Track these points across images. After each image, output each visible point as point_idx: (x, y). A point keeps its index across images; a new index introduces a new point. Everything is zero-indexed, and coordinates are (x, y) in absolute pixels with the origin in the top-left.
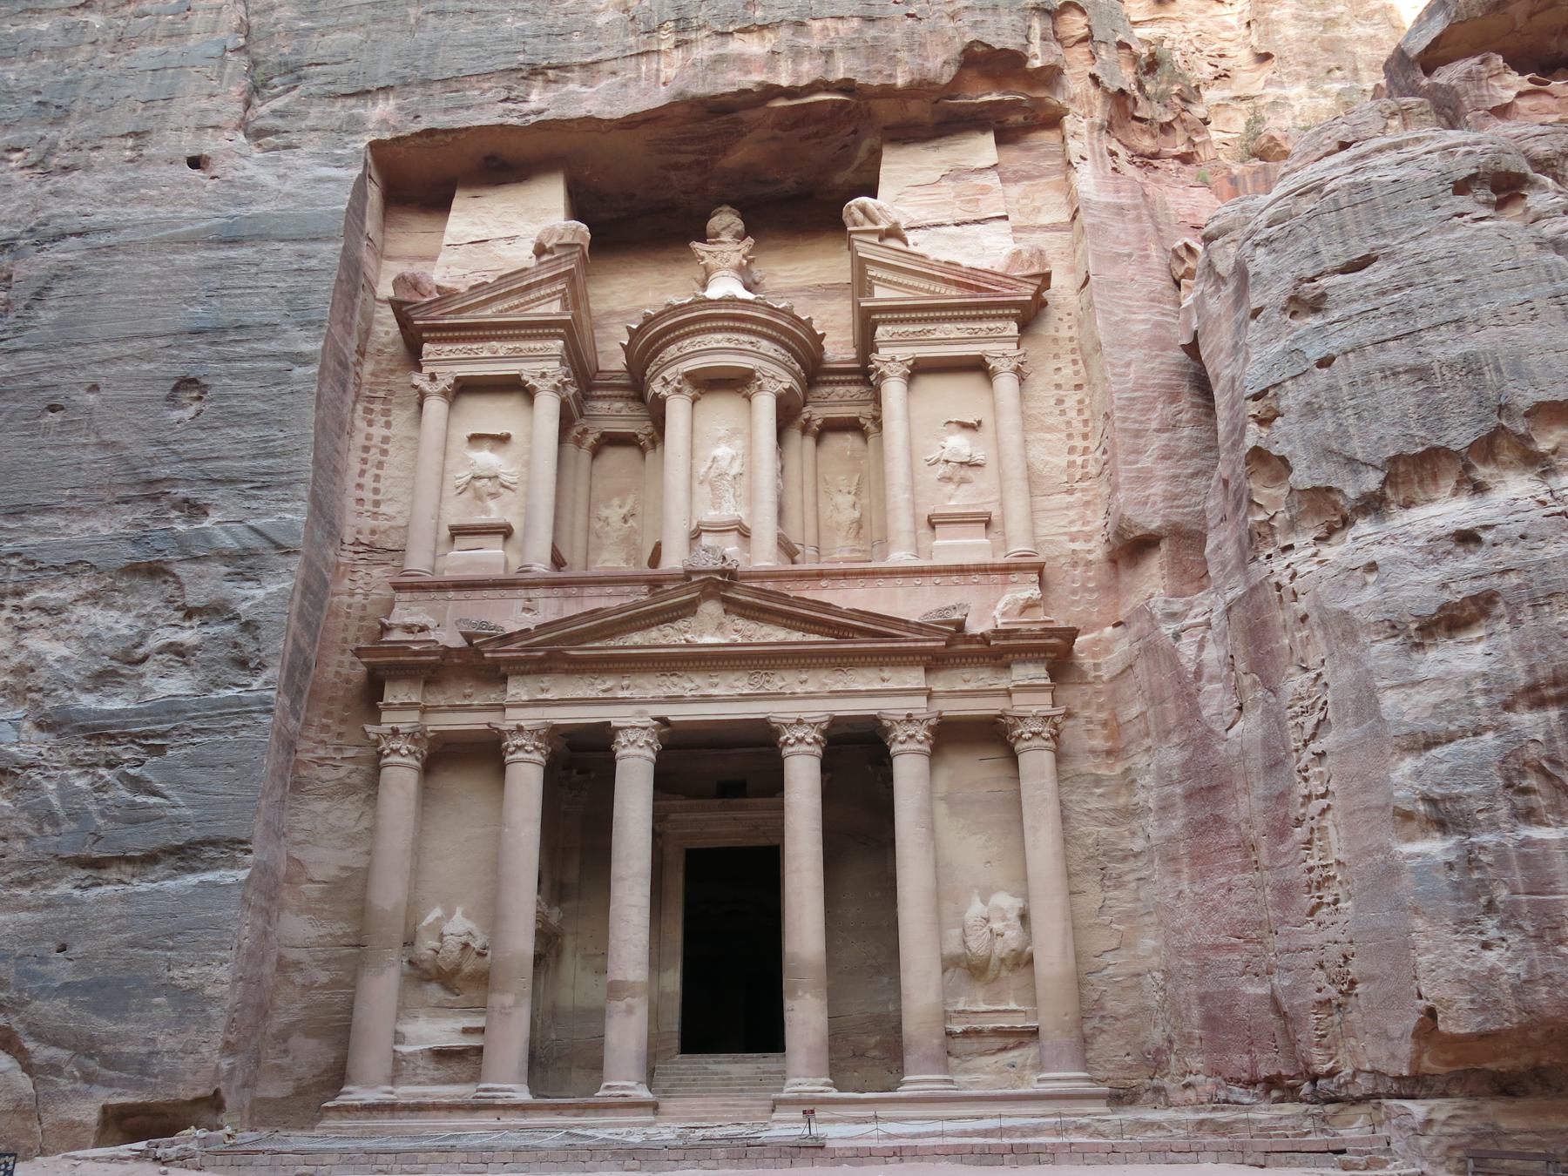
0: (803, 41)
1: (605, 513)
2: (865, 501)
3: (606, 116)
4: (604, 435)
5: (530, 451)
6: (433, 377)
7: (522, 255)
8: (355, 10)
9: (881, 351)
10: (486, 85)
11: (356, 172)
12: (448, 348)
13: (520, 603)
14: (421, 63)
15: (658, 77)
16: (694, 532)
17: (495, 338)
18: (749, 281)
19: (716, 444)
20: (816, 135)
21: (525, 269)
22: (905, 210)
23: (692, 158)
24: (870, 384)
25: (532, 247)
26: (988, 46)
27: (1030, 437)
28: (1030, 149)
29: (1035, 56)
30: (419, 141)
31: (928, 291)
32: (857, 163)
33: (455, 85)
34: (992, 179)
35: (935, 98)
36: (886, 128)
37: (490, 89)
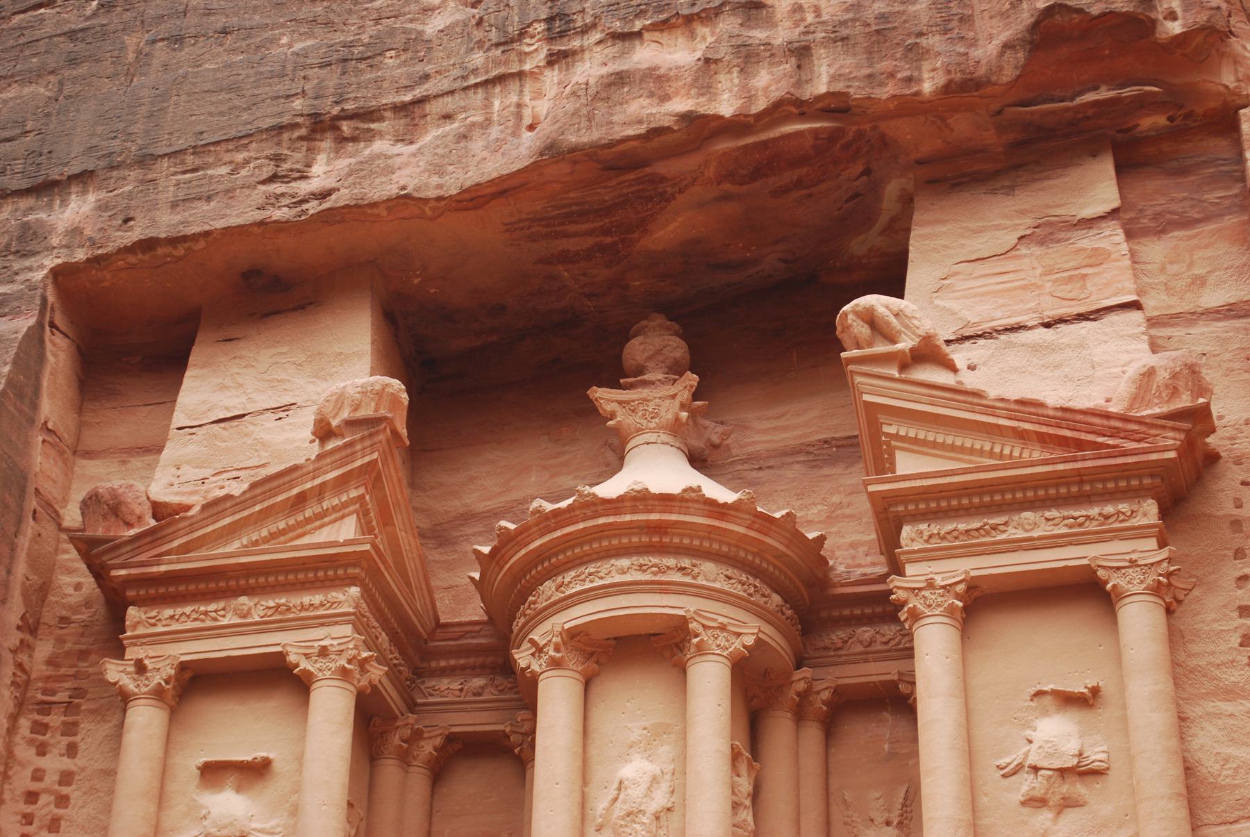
0: (758, 35)
3: (432, 193)
4: (451, 738)
5: (297, 788)
6: (141, 668)
7: (293, 442)
8: (42, 46)
9: (910, 569)
10: (240, 157)
11: (25, 323)
12: (168, 612)
14: (137, 128)
15: (519, 117)
17: (249, 591)
18: (697, 443)
19: (625, 758)
20: (799, 184)
21: (295, 468)
23: (590, 241)
25: (311, 428)
26: (1079, 11)
27: (1194, 711)
28: (1184, 172)
29: (1172, 16)
30: (132, 259)
32: (883, 220)
33: (190, 160)
34: (1113, 238)
35: (995, 107)
36: (919, 162)
37: (247, 162)
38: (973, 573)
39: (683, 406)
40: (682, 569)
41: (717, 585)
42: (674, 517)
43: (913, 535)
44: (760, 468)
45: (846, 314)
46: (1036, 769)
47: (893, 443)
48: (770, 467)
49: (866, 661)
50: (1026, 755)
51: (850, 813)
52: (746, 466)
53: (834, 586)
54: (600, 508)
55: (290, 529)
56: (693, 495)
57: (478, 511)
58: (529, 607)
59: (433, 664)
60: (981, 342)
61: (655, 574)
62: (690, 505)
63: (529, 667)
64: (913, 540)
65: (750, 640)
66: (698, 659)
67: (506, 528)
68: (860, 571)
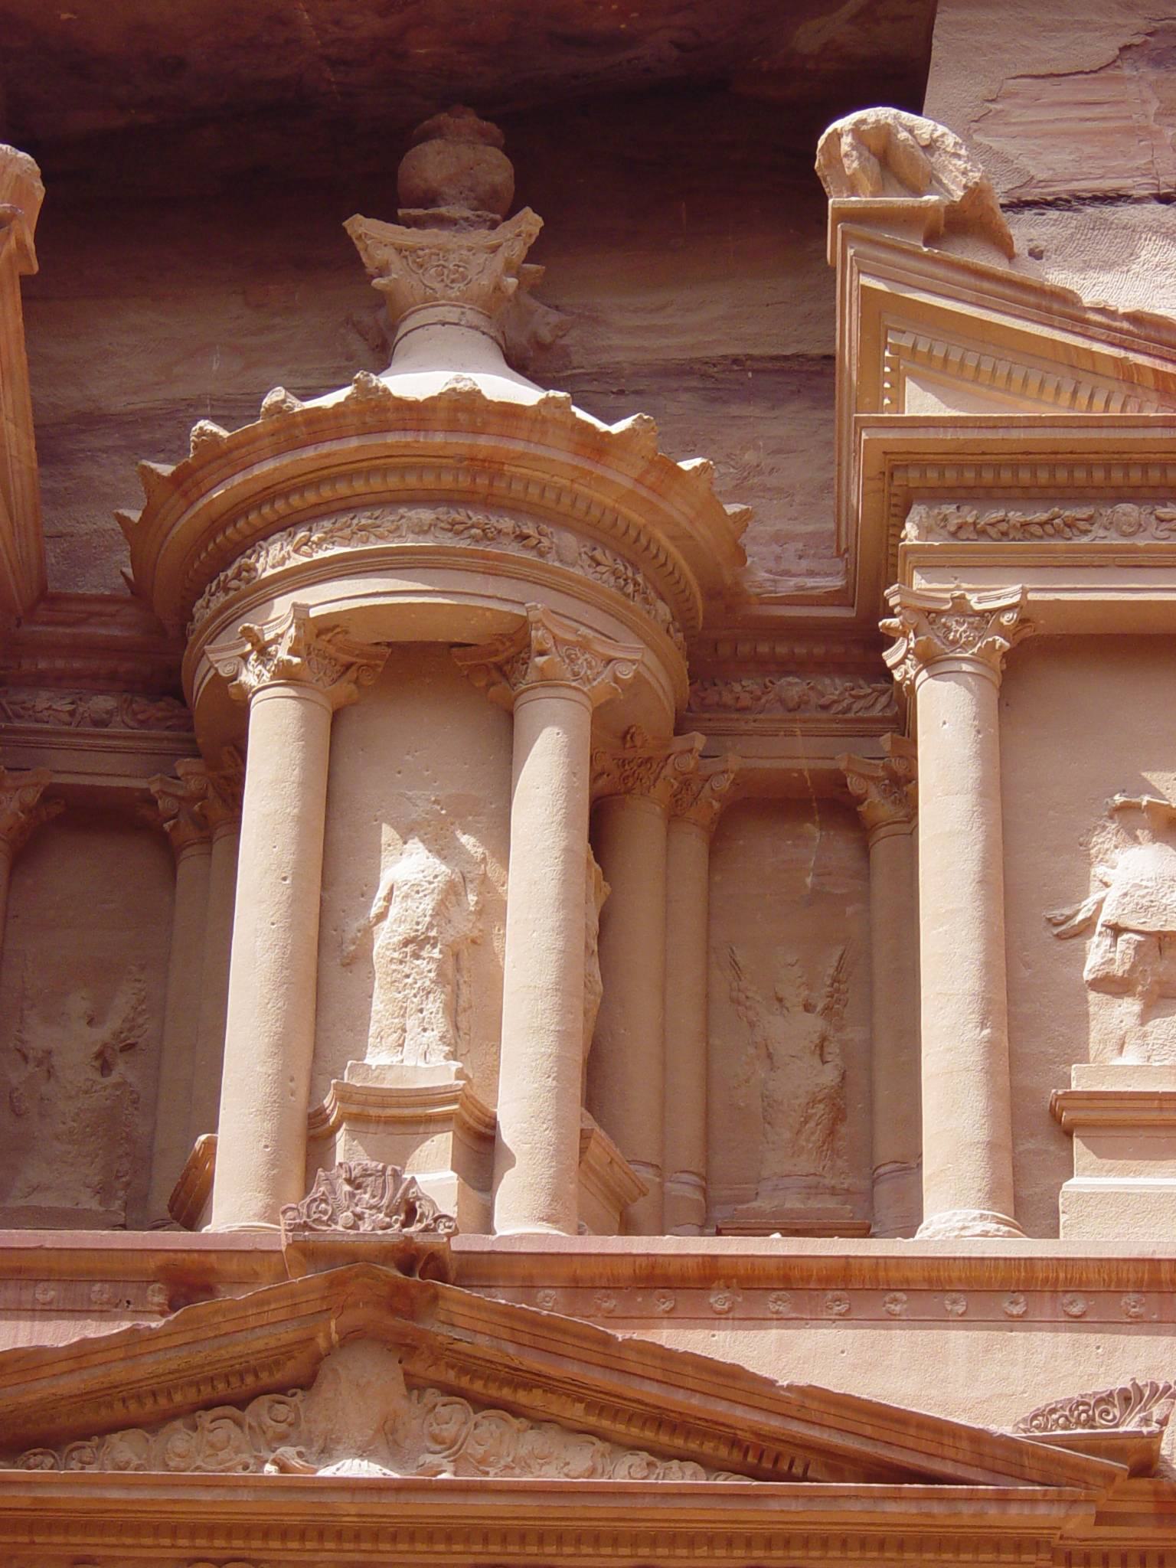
1: (40, 1036)
2: (855, 1034)
4: (50, 794)
22: (1010, 148)
24: (887, 674)
38: (1031, 596)
39: (509, 268)
40: (523, 537)
41: (577, 571)
42: (519, 447)
44: (621, 392)
45: (837, 135)
46: (1117, 930)
48: (638, 393)
49: (791, 734)
50: (1100, 904)
52: (595, 386)
58: (237, 576)
59: (26, 665)
60: (1053, 214)
61: (476, 539)
63: (235, 678)
65: (626, 673)
66: (542, 692)
67: (214, 435)
68: (793, 582)
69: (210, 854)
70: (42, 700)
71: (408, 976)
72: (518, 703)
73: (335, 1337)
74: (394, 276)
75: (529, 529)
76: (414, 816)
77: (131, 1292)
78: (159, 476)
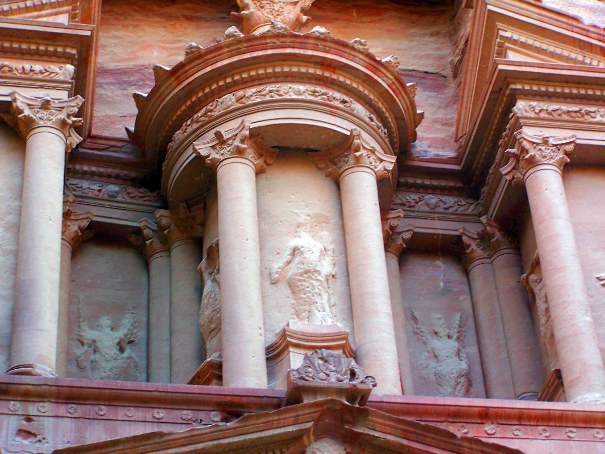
1: (89, 334)
4: (93, 225)
13: (14, 423)
16: (269, 349)
31: (583, 62)
39: (304, 11)
40: (344, 102)
43: (527, 108)
47: (507, 44)
49: (433, 219)
51: (419, 326)
53: (413, 160)
54: (289, 40)
55: (11, 12)
56: (361, 47)
57: (109, 68)
58: (205, 115)
59: (78, 167)
62: (357, 54)
63: (208, 156)
64: (526, 111)
68: (433, 153)
69: (170, 256)
70: (85, 184)
71: (308, 287)
72: (343, 175)
73: (312, 437)
74: (251, 10)
75: (346, 98)
76: (299, 221)
77: (202, 415)
78: (164, 70)
